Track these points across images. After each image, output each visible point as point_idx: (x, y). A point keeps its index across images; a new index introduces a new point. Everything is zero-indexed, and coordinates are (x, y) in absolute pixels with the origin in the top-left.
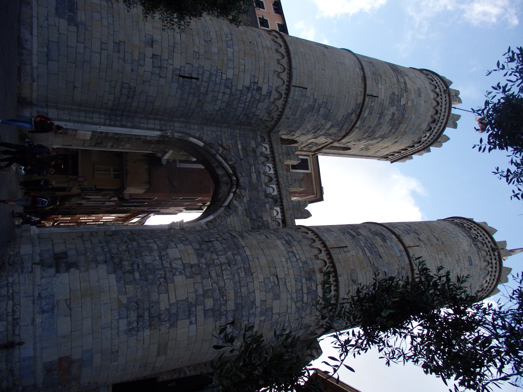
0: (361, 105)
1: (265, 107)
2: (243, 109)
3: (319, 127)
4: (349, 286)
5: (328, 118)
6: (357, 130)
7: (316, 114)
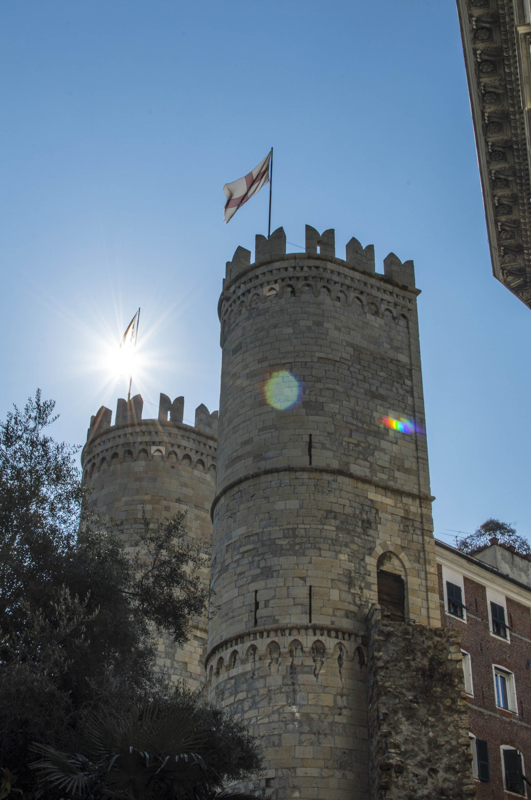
4: (233, 617)
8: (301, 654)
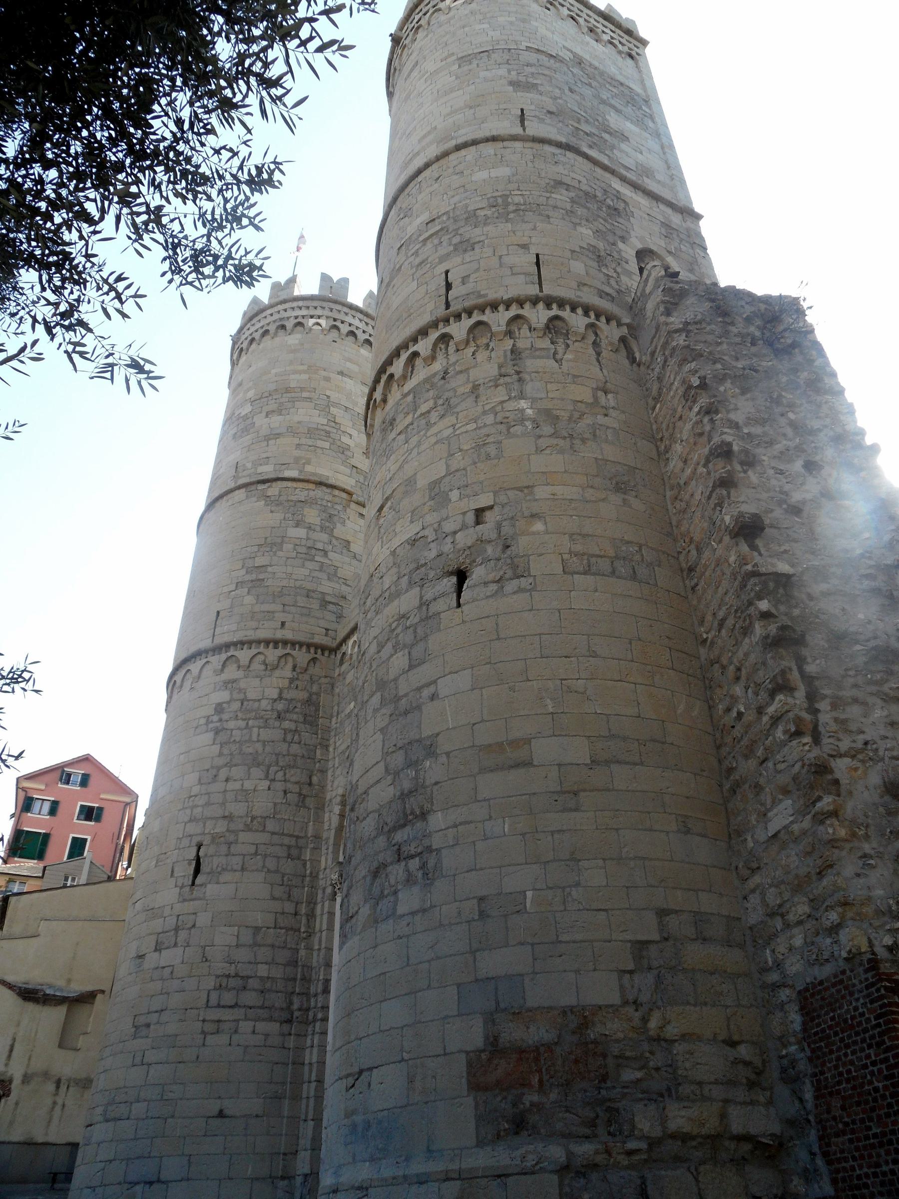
0: (249, 488)
1: (257, 682)
2: (265, 727)
3: (304, 550)
5: (279, 540)
6: (309, 468)
7: (270, 569)
8: (528, 334)
